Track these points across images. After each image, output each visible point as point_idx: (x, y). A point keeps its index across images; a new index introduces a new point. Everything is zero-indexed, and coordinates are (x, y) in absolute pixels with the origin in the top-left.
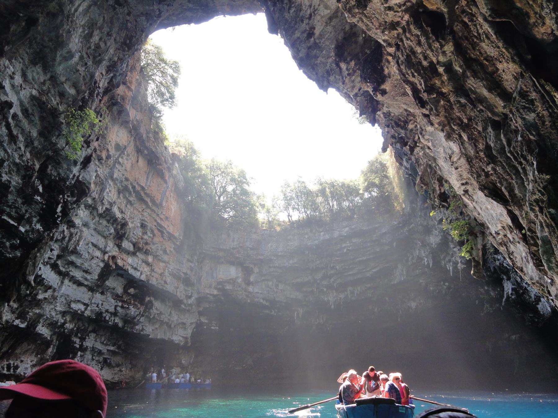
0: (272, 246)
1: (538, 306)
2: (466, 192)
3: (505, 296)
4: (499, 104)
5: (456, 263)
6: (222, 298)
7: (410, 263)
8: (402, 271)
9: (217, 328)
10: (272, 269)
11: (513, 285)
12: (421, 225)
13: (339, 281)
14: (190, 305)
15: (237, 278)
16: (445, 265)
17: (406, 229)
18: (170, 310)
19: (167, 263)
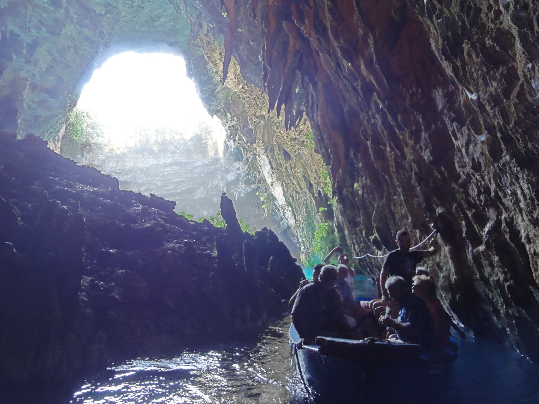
2: (272, 185)
4: (299, 189)
17: (213, 167)
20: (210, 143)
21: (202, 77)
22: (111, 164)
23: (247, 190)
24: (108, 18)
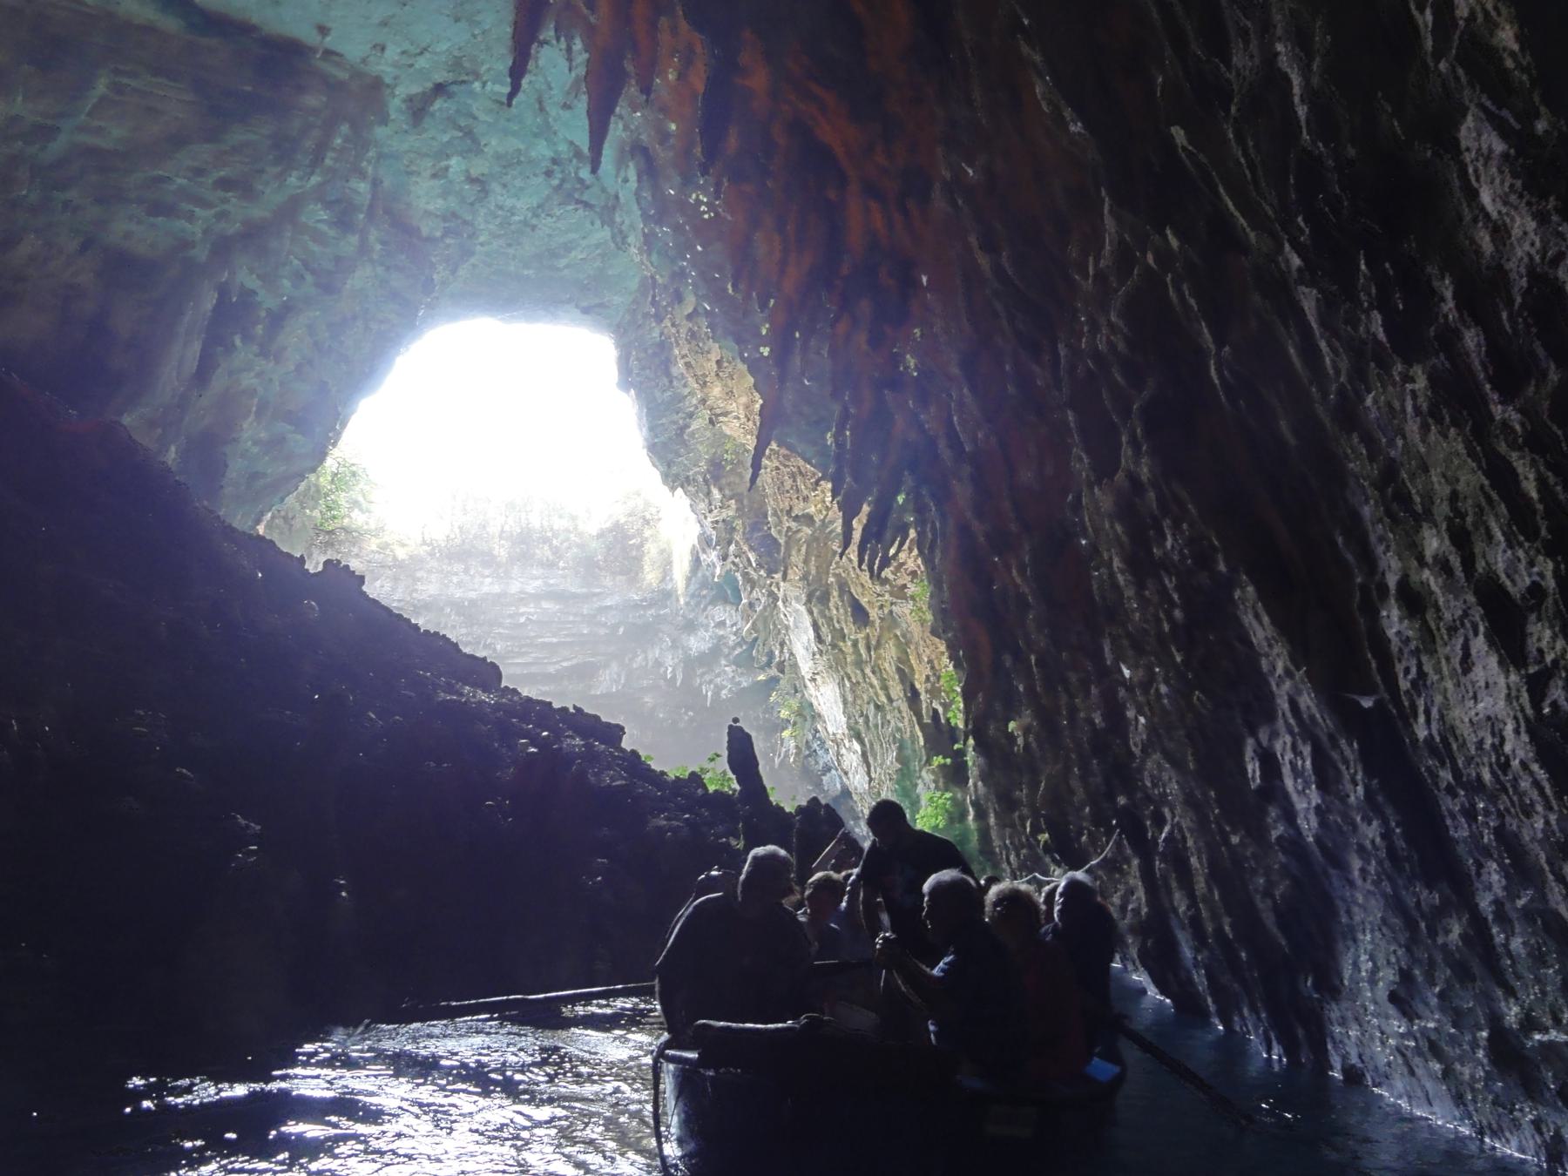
2: (814, 680)
4: (884, 699)
5: (718, 689)
20: (651, 549)
21: (658, 394)
22: (378, 584)
23: (739, 683)
24: (448, 246)
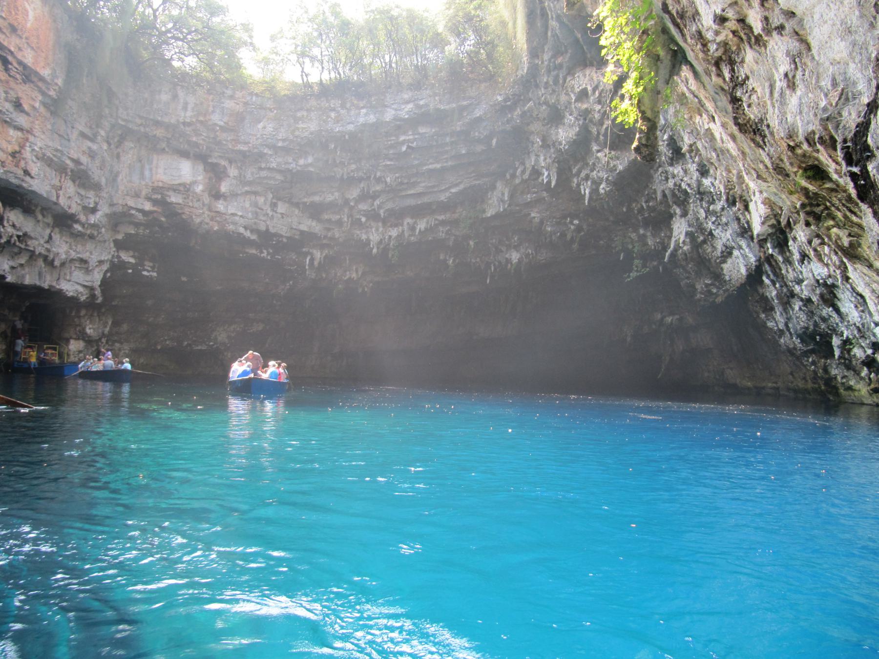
0: (264, 127)
1: (724, 266)
3: (672, 246)
5: (596, 183)
6: (163, 219)
7: (517, 181)
8: (503, 194)
9: (155, 274)
10: (264, 174)
11: (689, 226)
12: (546, 103)
13: (389, 205)
14: (94, 226)
15: (194, 183)
16: (579, 185)
17: (518, 111)
18: (48, 231)
19: (28, 132)
22: (260, 126)
23: (614, 168)
